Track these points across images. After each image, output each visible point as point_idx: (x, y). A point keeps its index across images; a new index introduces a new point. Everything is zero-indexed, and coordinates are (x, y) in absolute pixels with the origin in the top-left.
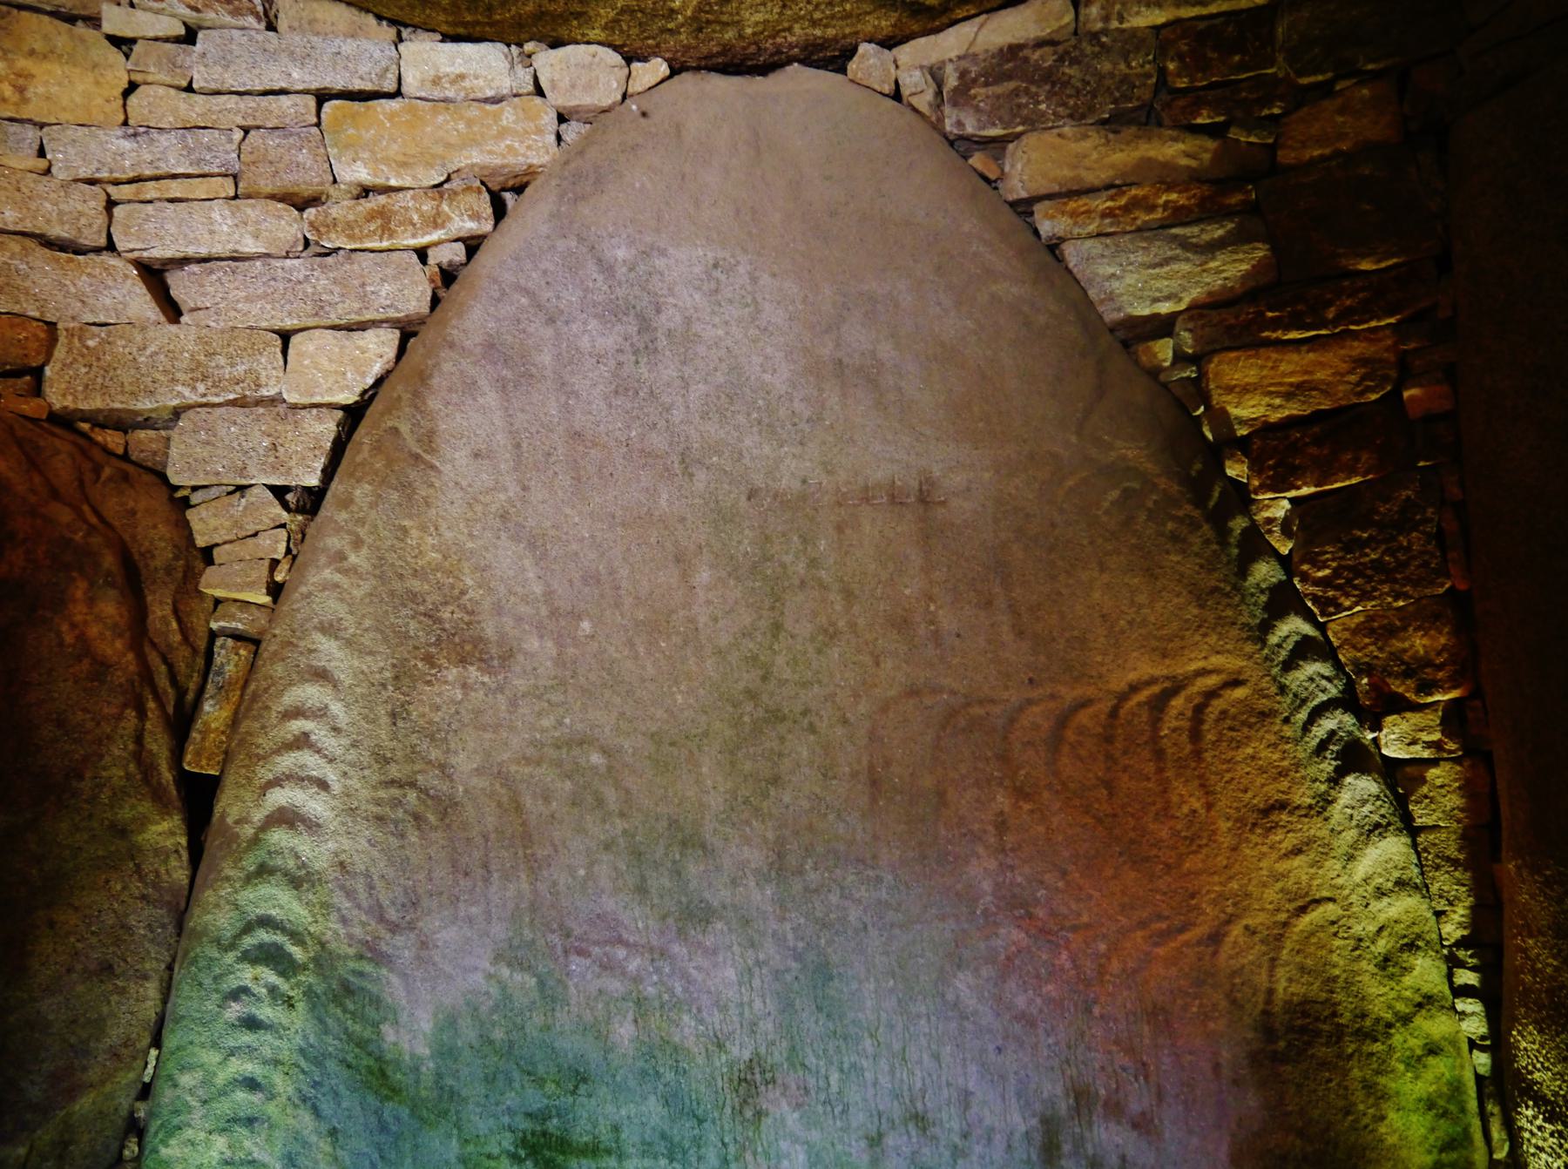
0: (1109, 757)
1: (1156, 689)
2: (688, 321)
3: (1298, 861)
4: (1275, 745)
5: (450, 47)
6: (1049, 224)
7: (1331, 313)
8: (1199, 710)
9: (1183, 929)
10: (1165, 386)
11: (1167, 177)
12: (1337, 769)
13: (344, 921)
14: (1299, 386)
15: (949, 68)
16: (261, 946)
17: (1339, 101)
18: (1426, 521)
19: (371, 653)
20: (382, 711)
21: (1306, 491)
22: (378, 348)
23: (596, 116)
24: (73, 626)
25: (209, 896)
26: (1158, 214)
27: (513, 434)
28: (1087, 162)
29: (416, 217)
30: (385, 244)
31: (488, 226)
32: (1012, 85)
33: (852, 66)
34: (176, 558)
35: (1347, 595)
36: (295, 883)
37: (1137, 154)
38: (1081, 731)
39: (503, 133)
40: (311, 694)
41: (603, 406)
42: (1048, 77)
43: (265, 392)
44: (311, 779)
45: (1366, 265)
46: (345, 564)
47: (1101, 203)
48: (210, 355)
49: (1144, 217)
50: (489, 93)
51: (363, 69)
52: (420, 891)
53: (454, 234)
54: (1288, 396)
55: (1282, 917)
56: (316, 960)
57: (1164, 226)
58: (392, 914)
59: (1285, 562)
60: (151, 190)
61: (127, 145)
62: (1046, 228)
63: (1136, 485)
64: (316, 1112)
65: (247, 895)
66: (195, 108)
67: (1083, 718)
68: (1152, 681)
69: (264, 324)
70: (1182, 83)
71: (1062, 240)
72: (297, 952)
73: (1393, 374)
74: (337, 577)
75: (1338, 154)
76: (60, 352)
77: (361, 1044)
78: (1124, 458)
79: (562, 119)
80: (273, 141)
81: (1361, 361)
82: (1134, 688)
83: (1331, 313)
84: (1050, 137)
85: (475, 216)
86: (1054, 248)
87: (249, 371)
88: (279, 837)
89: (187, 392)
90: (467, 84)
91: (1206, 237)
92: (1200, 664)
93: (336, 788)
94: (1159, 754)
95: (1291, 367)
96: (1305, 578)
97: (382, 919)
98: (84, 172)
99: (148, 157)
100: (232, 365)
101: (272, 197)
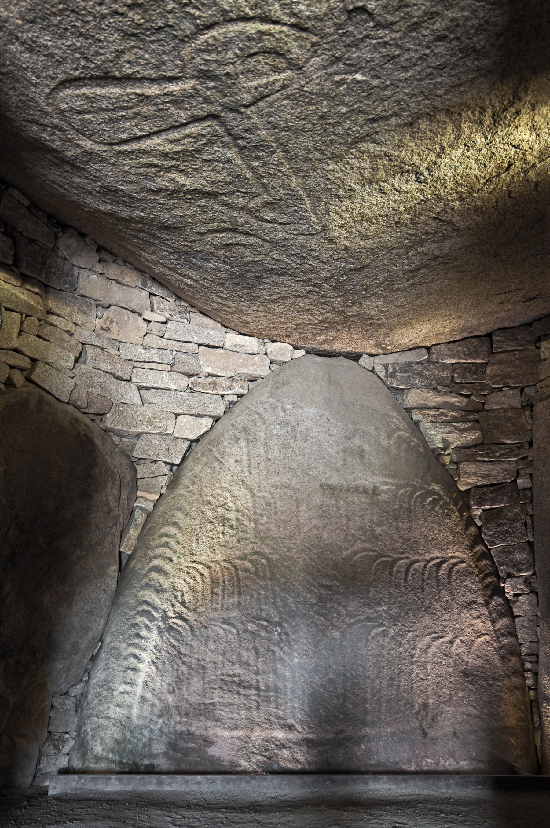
0: (423, 580)
1: (438, 560)
2: (307, 429)
3: (478, 621)
4: (473, 583)
5: (241, 337)
6: (416, 416)
7: (497, 454)
8: (451, 569)
9: (441, 637)
10: (447, 470)
11: (452, 407)
12: (491, 594)
13: (173, 605)
14: (487, 475)
15: (390, 366)
16: (144, 611)
17: (504, 393)
18: (522, 519)
19: (194, 519)
20: (194, 538)
21: (487, 507)
22: (206, 423)
23: (281, 364)
24: (106, 495)
25: (128, 592)
26: (449, 418)
27: (249, 456)
28: (429, 400)
29: (224, 386)
30: (214, 392)
31: (246, 392)
32: (408, 374)
33: (361, 361)
34: (131, 480)
35: (498, 540)
36: (158, 591)
37: (444, 400)
38: (416, 570)
39: (254, 364)
41: (278, 451)
42: (420, 374)
43: (168, 432)
44: (166, 557)
45: (508, 442)
46: (188, 489)
47: (432, 413)
48: (154, 418)
49: (444, 418)
50: (251, 352)
51: (215, 340)
52: (199, 598)
53: (235, 392)
54: (483, 478)
55: (473, 638)
56: (162, 617)
57: (450, 422)
58: (188, 605)
59: (479, 528)
60: (146, 365)
61: (143, 351)
62: (415, 417)
63: (437, 497)
64: (157, 668)
65: (142, 593)
66: (163, 343)
67: (416, 566)
68: (438, 558)
69: (172, 411)
70: (458, 381)
71: (420, 422)
72: (155, 614)
73: (515, 475)
74: (186, 493)
75: (502, 408)
76: (112, 410)
77: (174, 646)
78: (434, 489)
79: (271, 363)
80: (184, 356)
81: (506, 470)
82: (432, 559)
83: (497, 454)
84: (418, 391)
85: (243, 388)
86: (417, 423)
87: (165, 425)
88: (154, 575)
89: (145, 428)
90: (244, 348)
91: (462, 427)
92: (453, 555)
93: (175, 561)
94: (438, 581)
95: (485, 468)
96: (485, 534)
97: (185, 607)
98: (129, 358)
99: (148, 356)
100: (160, 422)
101: (181, 373)
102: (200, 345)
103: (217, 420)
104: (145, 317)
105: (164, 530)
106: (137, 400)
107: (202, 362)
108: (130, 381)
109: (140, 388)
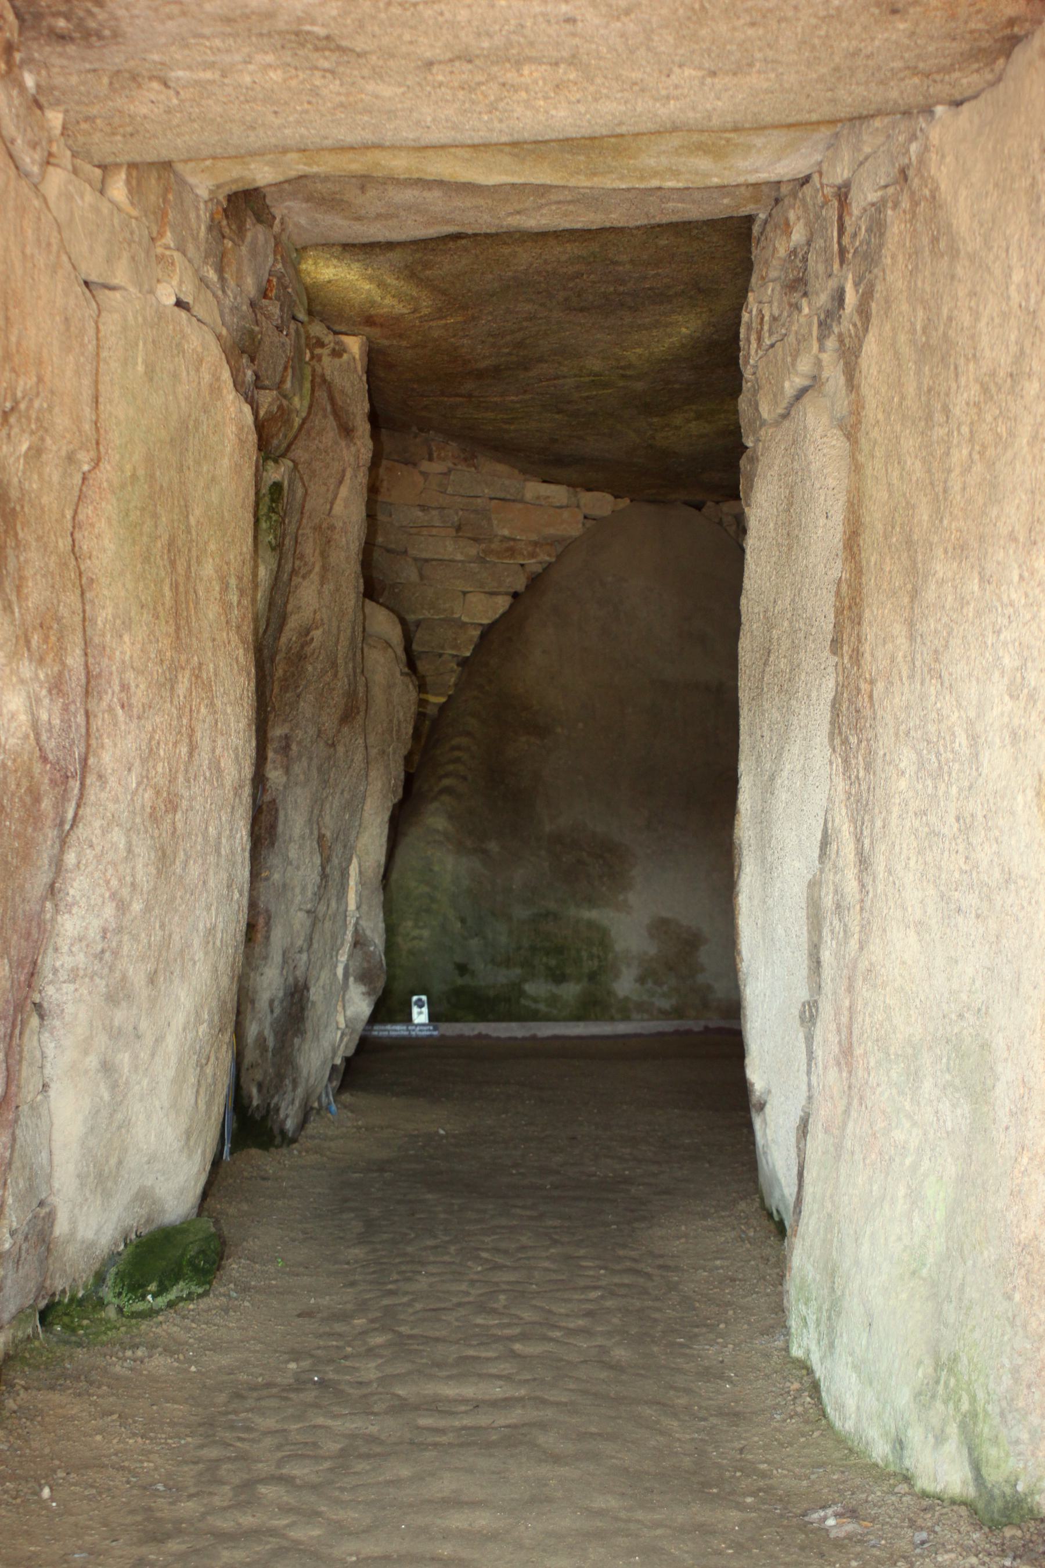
5: (545, 485)
22: (502, 603)
33: (704, 510)
40: (464, 741)
61: (420, 514)
79: (585, 517)
85: (549, 555)
102: (491, 499)
103: (515, 595)
104: (422, 469)
105: (455, 742)
106: (414, 577)
107: (495, 522)
108: (406, 552)
109: (415, 559)
